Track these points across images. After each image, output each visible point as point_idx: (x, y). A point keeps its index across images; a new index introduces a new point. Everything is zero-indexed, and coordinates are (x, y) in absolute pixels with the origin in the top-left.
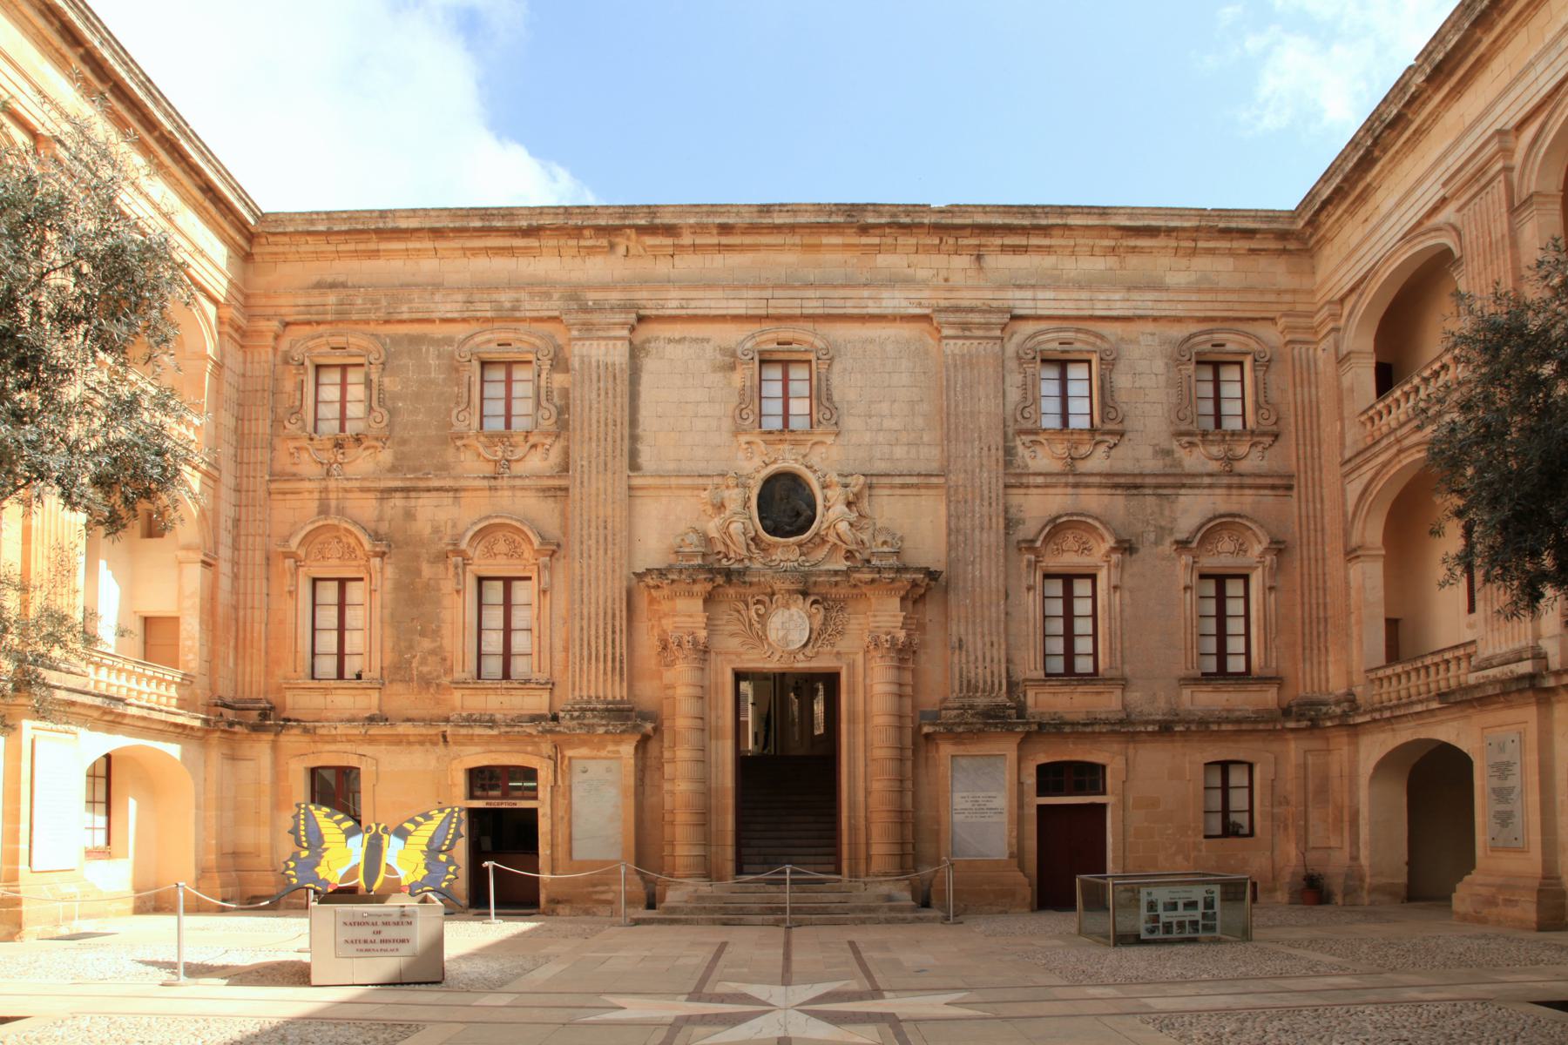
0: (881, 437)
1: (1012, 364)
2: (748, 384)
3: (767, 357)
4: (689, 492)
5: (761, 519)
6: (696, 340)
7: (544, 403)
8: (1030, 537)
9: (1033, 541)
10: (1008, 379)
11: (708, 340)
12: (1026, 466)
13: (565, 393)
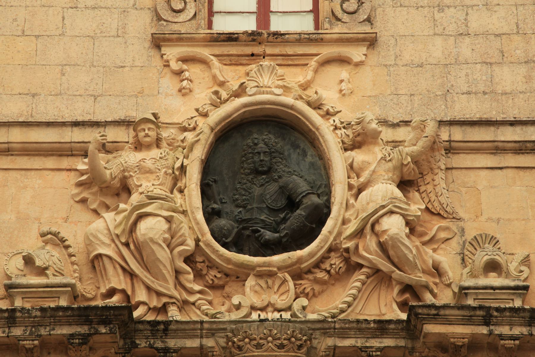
4: (50, 162)
5: (210, 215)
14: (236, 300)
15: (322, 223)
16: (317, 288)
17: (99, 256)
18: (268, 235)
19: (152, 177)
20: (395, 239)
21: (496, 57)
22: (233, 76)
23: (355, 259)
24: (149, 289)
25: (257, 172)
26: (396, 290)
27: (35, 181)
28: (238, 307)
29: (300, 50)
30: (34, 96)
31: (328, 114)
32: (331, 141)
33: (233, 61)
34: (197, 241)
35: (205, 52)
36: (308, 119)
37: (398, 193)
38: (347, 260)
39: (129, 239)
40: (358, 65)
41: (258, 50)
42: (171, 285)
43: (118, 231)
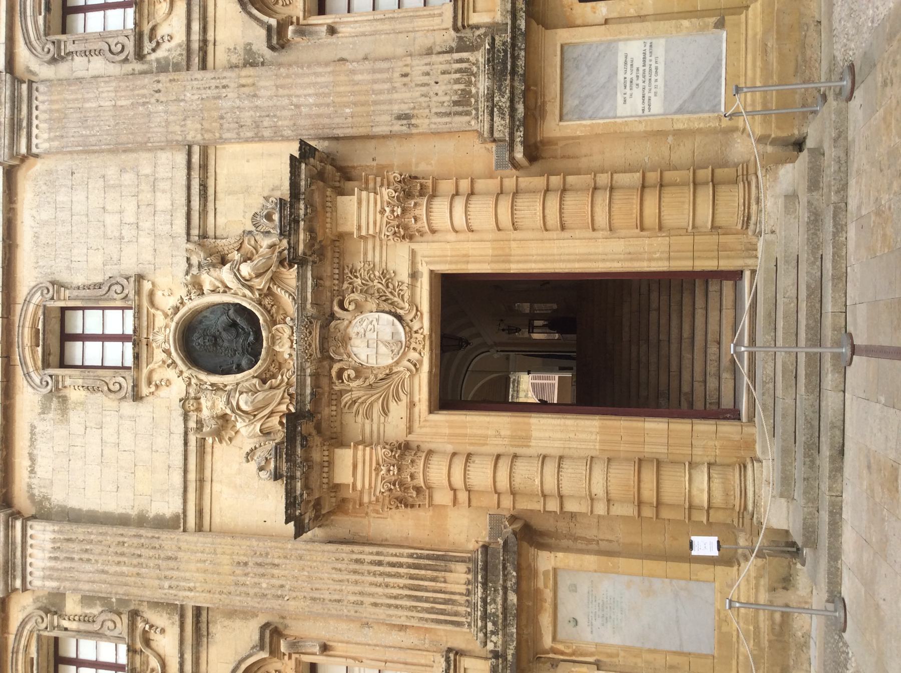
0: (146, 225)
1: (63, 70)
2: (80, 382)
3: (54, 359)
4: (208, 458)
5: (240, 370)
6: (32, 441)
7: (96, 627)
8: (263, 33)
9: (269, 29)
10: (80, 74)
11: (33, 427)
12: (180, 45)
13: (87, 600)
14: (287, 356)
15: (244, 309)
16: (281, 312)
17: (261, 431)
18: (251, 338)
19: (217, 402)
20: (253, 269)
21: (151, 209)
22: (159, 355)
23: (265, 291)
24: (279, 404)
25: (215, 344)
26: (283, 269)
27: (218, 466)
28: (290, 355)
29: (145, 318)
30: (169, 467)
31: (182, 303)
32: (198, 302)
33: (150, 356)
34: (254, 377)
35: (145, 371)
36: (184, 315)
37: (228, 265)
38: (266, 295)
39: (251, 415)
40: (153, 284)
41: (144, 341)
42: (278, 391)
43: (247, 420)
